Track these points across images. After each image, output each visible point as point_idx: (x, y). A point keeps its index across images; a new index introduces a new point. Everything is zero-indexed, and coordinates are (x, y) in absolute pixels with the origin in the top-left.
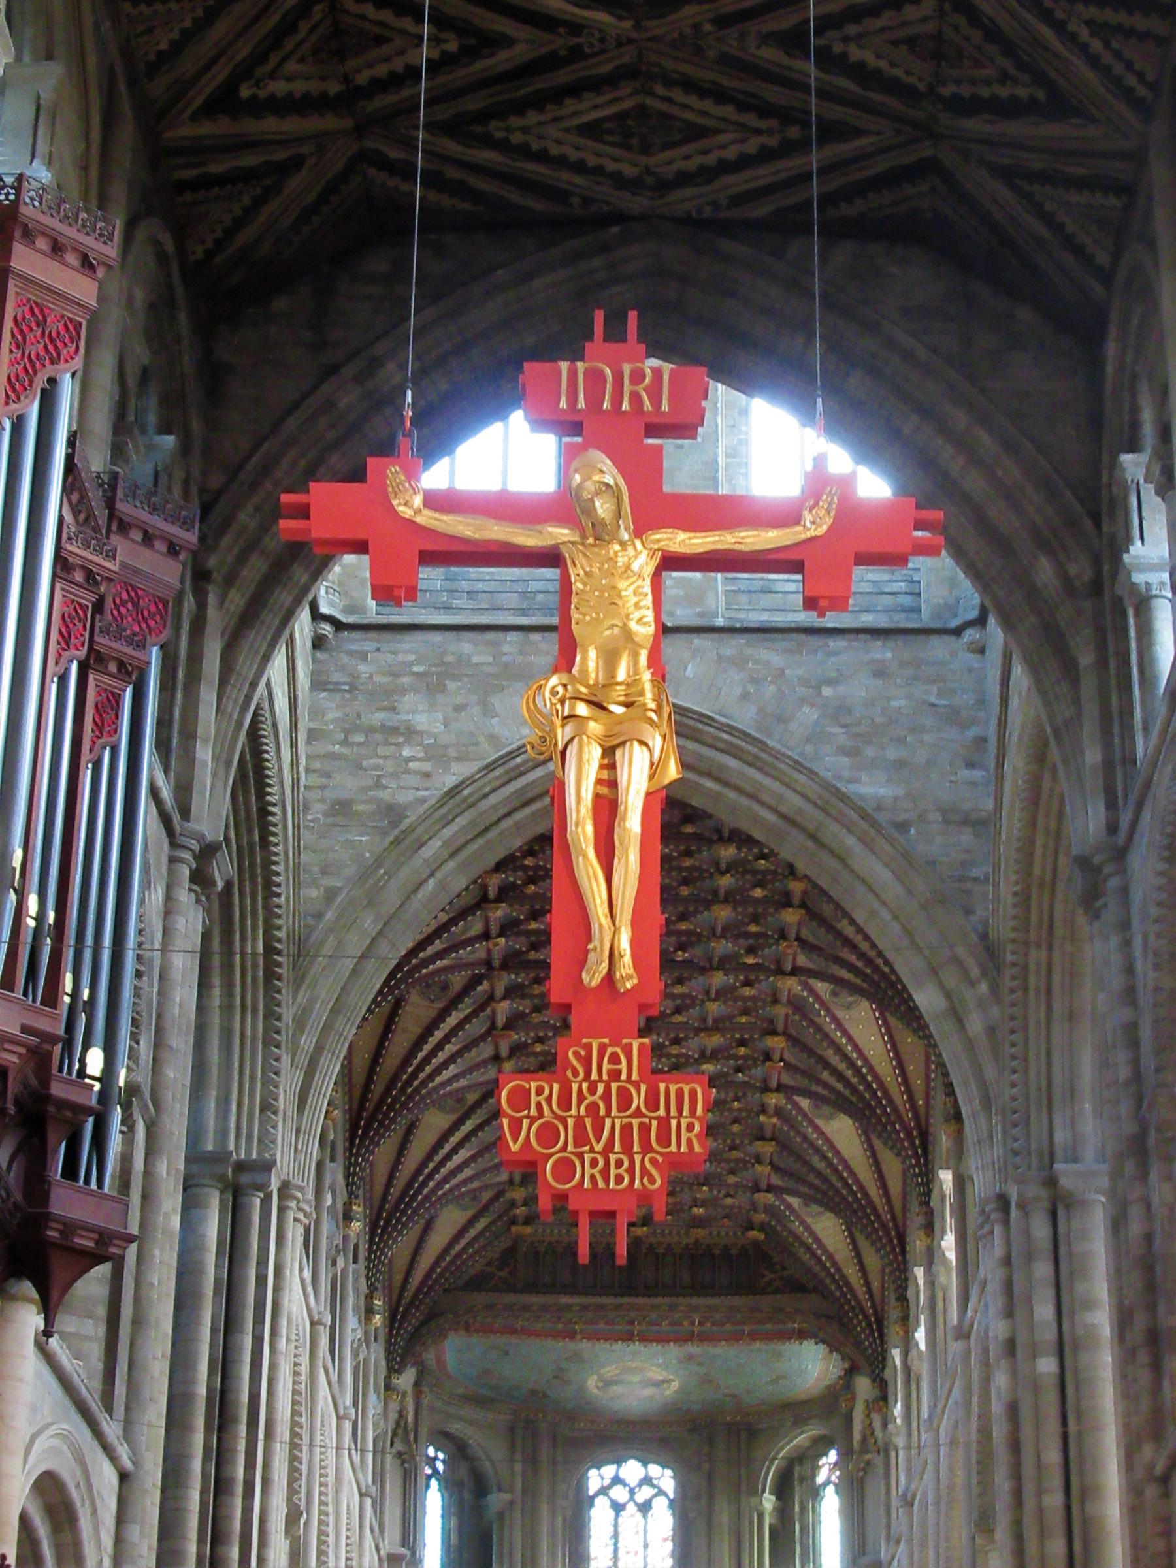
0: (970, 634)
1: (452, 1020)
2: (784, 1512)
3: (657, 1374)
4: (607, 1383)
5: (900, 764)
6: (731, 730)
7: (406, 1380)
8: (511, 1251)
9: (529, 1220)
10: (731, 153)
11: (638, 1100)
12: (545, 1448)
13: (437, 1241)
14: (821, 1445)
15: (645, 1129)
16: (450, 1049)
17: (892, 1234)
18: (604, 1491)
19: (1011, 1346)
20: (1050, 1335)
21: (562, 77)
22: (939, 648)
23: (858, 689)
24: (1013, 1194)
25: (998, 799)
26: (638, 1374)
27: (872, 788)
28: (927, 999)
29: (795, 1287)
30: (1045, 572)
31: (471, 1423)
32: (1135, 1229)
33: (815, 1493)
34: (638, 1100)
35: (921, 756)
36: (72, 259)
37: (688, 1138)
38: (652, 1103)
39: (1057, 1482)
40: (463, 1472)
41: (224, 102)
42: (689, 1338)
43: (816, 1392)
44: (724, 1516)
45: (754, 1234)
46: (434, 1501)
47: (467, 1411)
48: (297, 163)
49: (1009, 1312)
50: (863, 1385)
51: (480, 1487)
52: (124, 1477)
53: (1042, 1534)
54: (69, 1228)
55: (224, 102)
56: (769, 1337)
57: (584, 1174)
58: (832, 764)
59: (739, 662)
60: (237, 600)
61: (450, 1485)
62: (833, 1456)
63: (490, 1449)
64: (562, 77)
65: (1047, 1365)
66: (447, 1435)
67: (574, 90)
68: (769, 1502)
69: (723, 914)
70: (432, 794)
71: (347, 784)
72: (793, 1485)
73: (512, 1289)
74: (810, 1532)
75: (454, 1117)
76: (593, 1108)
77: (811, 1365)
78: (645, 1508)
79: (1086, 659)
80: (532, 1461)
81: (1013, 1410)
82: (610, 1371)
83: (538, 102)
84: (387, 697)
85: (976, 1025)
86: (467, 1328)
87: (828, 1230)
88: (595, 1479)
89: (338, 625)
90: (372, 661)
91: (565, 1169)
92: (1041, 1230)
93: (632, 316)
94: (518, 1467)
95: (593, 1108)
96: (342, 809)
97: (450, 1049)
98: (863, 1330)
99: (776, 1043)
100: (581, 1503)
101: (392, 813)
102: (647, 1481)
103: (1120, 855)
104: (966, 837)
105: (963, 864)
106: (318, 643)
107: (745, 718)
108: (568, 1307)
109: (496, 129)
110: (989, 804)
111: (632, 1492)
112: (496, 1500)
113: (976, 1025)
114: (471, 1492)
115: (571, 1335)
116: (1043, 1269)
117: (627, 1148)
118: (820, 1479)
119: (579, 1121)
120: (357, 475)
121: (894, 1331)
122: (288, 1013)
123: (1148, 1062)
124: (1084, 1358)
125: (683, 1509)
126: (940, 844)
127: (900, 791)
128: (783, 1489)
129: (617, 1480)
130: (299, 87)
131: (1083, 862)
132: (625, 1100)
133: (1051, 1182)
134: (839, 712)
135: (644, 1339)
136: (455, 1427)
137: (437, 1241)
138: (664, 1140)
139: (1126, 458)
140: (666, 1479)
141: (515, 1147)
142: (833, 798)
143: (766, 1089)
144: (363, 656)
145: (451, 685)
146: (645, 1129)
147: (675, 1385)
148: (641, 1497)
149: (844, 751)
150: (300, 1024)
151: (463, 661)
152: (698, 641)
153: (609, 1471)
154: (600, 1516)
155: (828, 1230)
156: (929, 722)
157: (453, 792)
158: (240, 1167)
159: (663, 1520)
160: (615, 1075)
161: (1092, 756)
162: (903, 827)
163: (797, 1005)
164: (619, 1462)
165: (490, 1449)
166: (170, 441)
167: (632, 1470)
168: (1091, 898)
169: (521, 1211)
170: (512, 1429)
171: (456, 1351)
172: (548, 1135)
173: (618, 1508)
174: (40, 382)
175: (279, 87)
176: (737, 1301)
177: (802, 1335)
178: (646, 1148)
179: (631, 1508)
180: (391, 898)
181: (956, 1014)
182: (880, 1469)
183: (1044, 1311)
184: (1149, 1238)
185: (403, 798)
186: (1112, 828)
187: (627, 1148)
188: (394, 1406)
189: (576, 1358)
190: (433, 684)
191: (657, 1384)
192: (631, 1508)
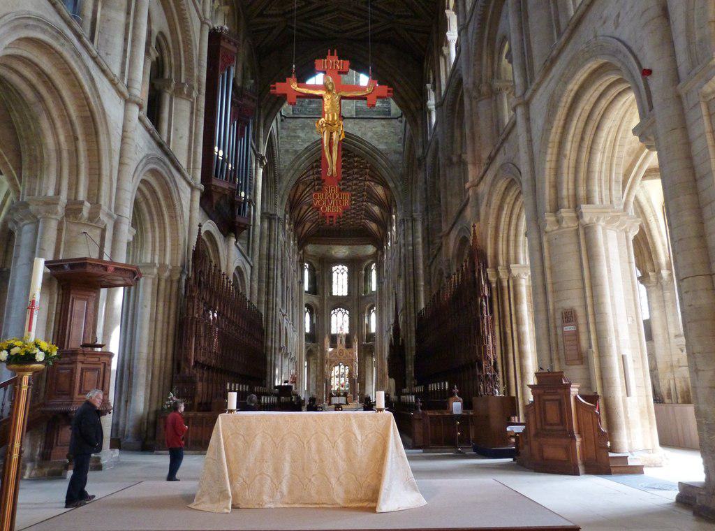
0: (399, 119)
1: (308, 189)
5: (386, 143)
6: (356, 136)
7: (301, 252)
9: (322, 225)
10: (355, 26)
11: (337, 197)
13: (306, 228)
14: (372, 263)
15: (338, 202)
16: (308, 194)
17: (384, 225)
19: (404, 245)
20: (411, 242)
21: (324, 10)
22: (394, 121)
23: (379, 129)
24: (405, 218)
25: (404, 148)
26: (341, 251)
27: (381, 147)
28: (391, 185)
30: (412, 106)
32: (426, 224)
33: (371, 271)
34: (337, 197)
35: (390, 142)
36: (232, 43)
37: (346, 203)
38: (340, 197)
39: (411, 267)
41: (261, 15)
42: (349, 245)
44: (356, 275)
46: (306, 273)
48: (275, 27)
49: (404, 239)
50: (380, 252)
52: (252, 267)
53: (410, 276)
54: (240, 223)
55: (261, 15)
56: (364, 244)
57: (328, 209)
58: (374, 143)
59: (357, 124)
60: (266, 112)
61: (309, 270)
62: (374, 264)
63: (316, 265)
64: (324, 10)
65: (411, 248)
67: (327, 13)
68: (363, 272)
69: (355, 170)
70: (303, 149)
71: (288, 146)
72: (368, 270)
76: (329, 198)
77: (371, 249)
78: (342, 273)
79: (420, 122)
81: (405, 255)
82: (336, 250)
83: (321, 15)
84: (294, 130)
85: (400, 189)
87: (373, 226)
88: (334, 268)
89: (285, 117)
90: (292, 124)
91: (324, 209)
92: (410, 225)
93: (335, 51)
95: (329, 198)
96: (287, 151)
97: (308, 194)
98: (379, 242)
99: (365, 193)
100: (331, 273)
101: (296, 151)
103: (425, 158)
104: (398, 156)
105: (398, 161)
106: (282, 120)
107: (359, 134)
109: (312, 20)
110: (402, 150)
112: (317, 272)
113: (400, 189)
114: (312, 270)
115: (329, 244)
116: (410, 231)
117: (335, 205)
118: (372, 268)
119: (327, 200)
120: (285, 81)
121: (385, 243)
122: (278, 188)
123: (429, 195)
124: (417, 246)
125: (348, 273)
126: (394, 157)
127: (386, 147)
130: (274, 12)
131: (419, 159)
132: (335, 196)
133: (412, 216)
134: (376, 133)
135: (343, 245)
136: (310, 260)
137: (306, 228)
138: (342, 203)
139: (427, 85)
140: (346, 268)
141: (315, 205)
142: (374, 149)
143: (363, 201)
144: (290, 123)
145: (306, 128)
146: (338, 202)
149: (376, 140)
150: (280, 189)
151: (308, 124)
152: (351, 120)
153: (336, 267)
154: (335, 275)
155: (373, 226)
156: (392, 135)
157: (308, 147)
158: (271, 215)
159: (346, 275)
160: (333, 192)
161: (420, 140)
162: (387, 154)
163: (368, 186)
165: (316, 265)
166: (252, 81)
167: (340, 267)
168: (420, 165)
169: (320, 223)
171: (310, 248)
172: (321, 202)
174: (227, 67)
175: (271, 12)
178: (339, 205)
180: (296, 167)
181: (396, 187)
183: (410, 239)
184: (428, 225)
185: (298, 149)
186: (423, 153)
187: (335, 205)
189: (331, 248)
190: (303, 128)
191: (345, 252)
192: (340, 274)
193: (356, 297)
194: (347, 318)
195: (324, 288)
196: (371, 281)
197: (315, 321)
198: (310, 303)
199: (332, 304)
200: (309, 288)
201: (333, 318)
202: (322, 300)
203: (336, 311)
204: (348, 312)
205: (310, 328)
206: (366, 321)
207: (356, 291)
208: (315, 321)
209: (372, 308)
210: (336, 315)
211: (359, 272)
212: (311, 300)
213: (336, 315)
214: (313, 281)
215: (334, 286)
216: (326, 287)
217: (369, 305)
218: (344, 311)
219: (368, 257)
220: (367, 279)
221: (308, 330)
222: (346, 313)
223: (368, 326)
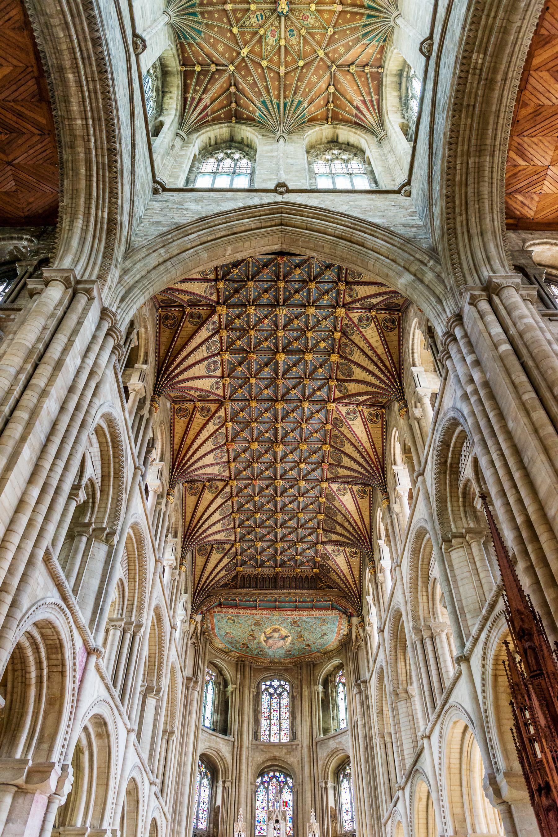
2: (326, 693)
3: (284, 632)
4: (268, 638)
7: (199, 618)
8: (236, 577)
12: (247, 670)
18: (266, 690)
29: (331, 588)
31: (224, 660)
40: (221, 680)
43: (335, 647)
44: (306, 693)
45: (316, 570)
47: (223, 656)
51: (226, 685)
61: (217, 684)
66: (215, 665)
68: (320, 688)
73: (235, 587)
74: (335, 699)
75: (214, 495)
78: (280, 695)
86: (220, 605)
88: (263, 687)
94: (238, 676)
102: (280, 686)
108: (254, 594)
111: (276, 690)
112: (230, 688)
118: (337, 680)
128: (325, 684)
129: (271, 686)
140: (287, 687)
148: (278, 692)
153: (268, 683)
154: (265, 698)
159: (285, 701)
164: (271, 680)
167: (276, 683)
170: (237, 664)
173: (271, 695)
176: (311, 591)
177: (332, 608)
179: (275, 696)
182: (364, 647)
188: (193, 626)
189: (257, 624)
192: (275, 696)
193: (306, 742)
194: (287, 796)
195: (242, 722)
196: (336, 707)
197: (219, 802)
198: (209, 752)
199: (260, 758)
200: (213, 723)
201: (261, 795)
202: (237, 748)
203: (266, 778)
204: (290, 781)
205: (209, 821)
206: (331, 803)
207: (306, 729)
208: (219, 802)
209: (341, 769)
210: (267, 789)
211: (309, 686)
212: (213, 745)
213: (267, 789)
214: (223, 706)
215: (264, 723)
216: (246, 718)
217: (333, 765)
218: (282, 779)
219: (328, 655)
220: (327, 703)
221: (203, 825)
222: (286, 783)
223: (335, 816)
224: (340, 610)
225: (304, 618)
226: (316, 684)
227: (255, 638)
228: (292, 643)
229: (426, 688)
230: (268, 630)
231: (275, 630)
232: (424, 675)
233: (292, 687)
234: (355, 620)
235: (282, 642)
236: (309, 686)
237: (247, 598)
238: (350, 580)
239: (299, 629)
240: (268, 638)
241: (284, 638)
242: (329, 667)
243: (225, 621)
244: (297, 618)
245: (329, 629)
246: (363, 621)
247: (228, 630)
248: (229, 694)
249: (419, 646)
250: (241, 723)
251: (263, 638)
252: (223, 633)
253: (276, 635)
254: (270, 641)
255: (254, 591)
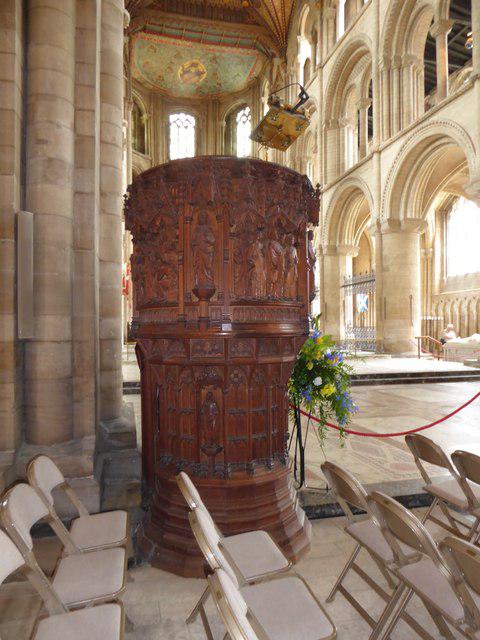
3: (201, 67)
14: (243, 107)
29: (258, 24)
40: (136, 110)
44: (211, 124)
51: (140, 114)
68: (224, 123)
72: (230, 120)
78: (186, 127)
80: (156, 106)
86: (144, 30)
108: (181, 21)
112: (145, 116)
140: (192, 120)
147: (204, 76)
154: (173, 128)
176: (240, 26)
177: (254, 47)
219: (235, 95)
224: (260, 50)
225: (224, 55)
226: (220, 120)
227: (172, 71)
228: (206, 81)
229: (385, 112)
230: (187, 65)
231: (194, 65)
232: (385, 102)
233: (198, 120)
234: (277, 61)
235: (197, 78)
236: (215, 120)
237: (175, 25)
238: (280, 18)
239: (216, 66)
240: (185, 72)
241: (199, 74)
242: (233, 106)
243: (146, 50)
244: (218, 54)
245: (237, 69)
246: (286, 62)
247: (149, 60)
248: (144, 122)
249: (385, 76)
250: (156, 146)
251: (180, 72)
252: (141, 62)
253: (193, 70)
254: (186, 76)
255: (181, 17)
